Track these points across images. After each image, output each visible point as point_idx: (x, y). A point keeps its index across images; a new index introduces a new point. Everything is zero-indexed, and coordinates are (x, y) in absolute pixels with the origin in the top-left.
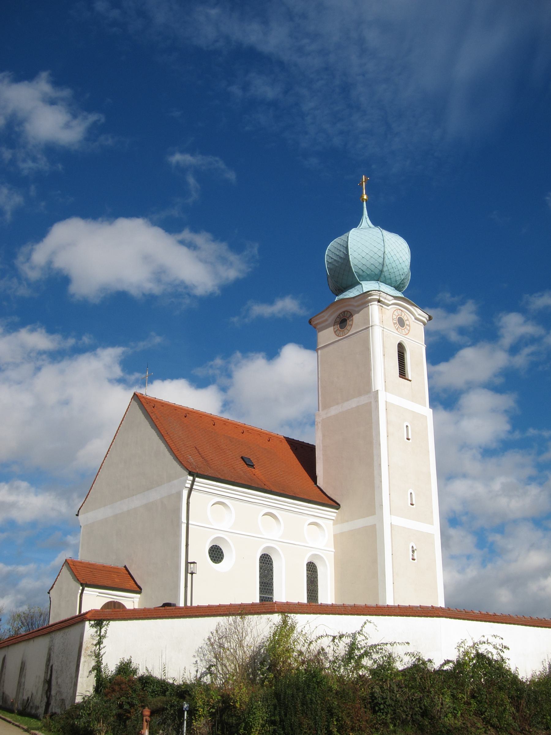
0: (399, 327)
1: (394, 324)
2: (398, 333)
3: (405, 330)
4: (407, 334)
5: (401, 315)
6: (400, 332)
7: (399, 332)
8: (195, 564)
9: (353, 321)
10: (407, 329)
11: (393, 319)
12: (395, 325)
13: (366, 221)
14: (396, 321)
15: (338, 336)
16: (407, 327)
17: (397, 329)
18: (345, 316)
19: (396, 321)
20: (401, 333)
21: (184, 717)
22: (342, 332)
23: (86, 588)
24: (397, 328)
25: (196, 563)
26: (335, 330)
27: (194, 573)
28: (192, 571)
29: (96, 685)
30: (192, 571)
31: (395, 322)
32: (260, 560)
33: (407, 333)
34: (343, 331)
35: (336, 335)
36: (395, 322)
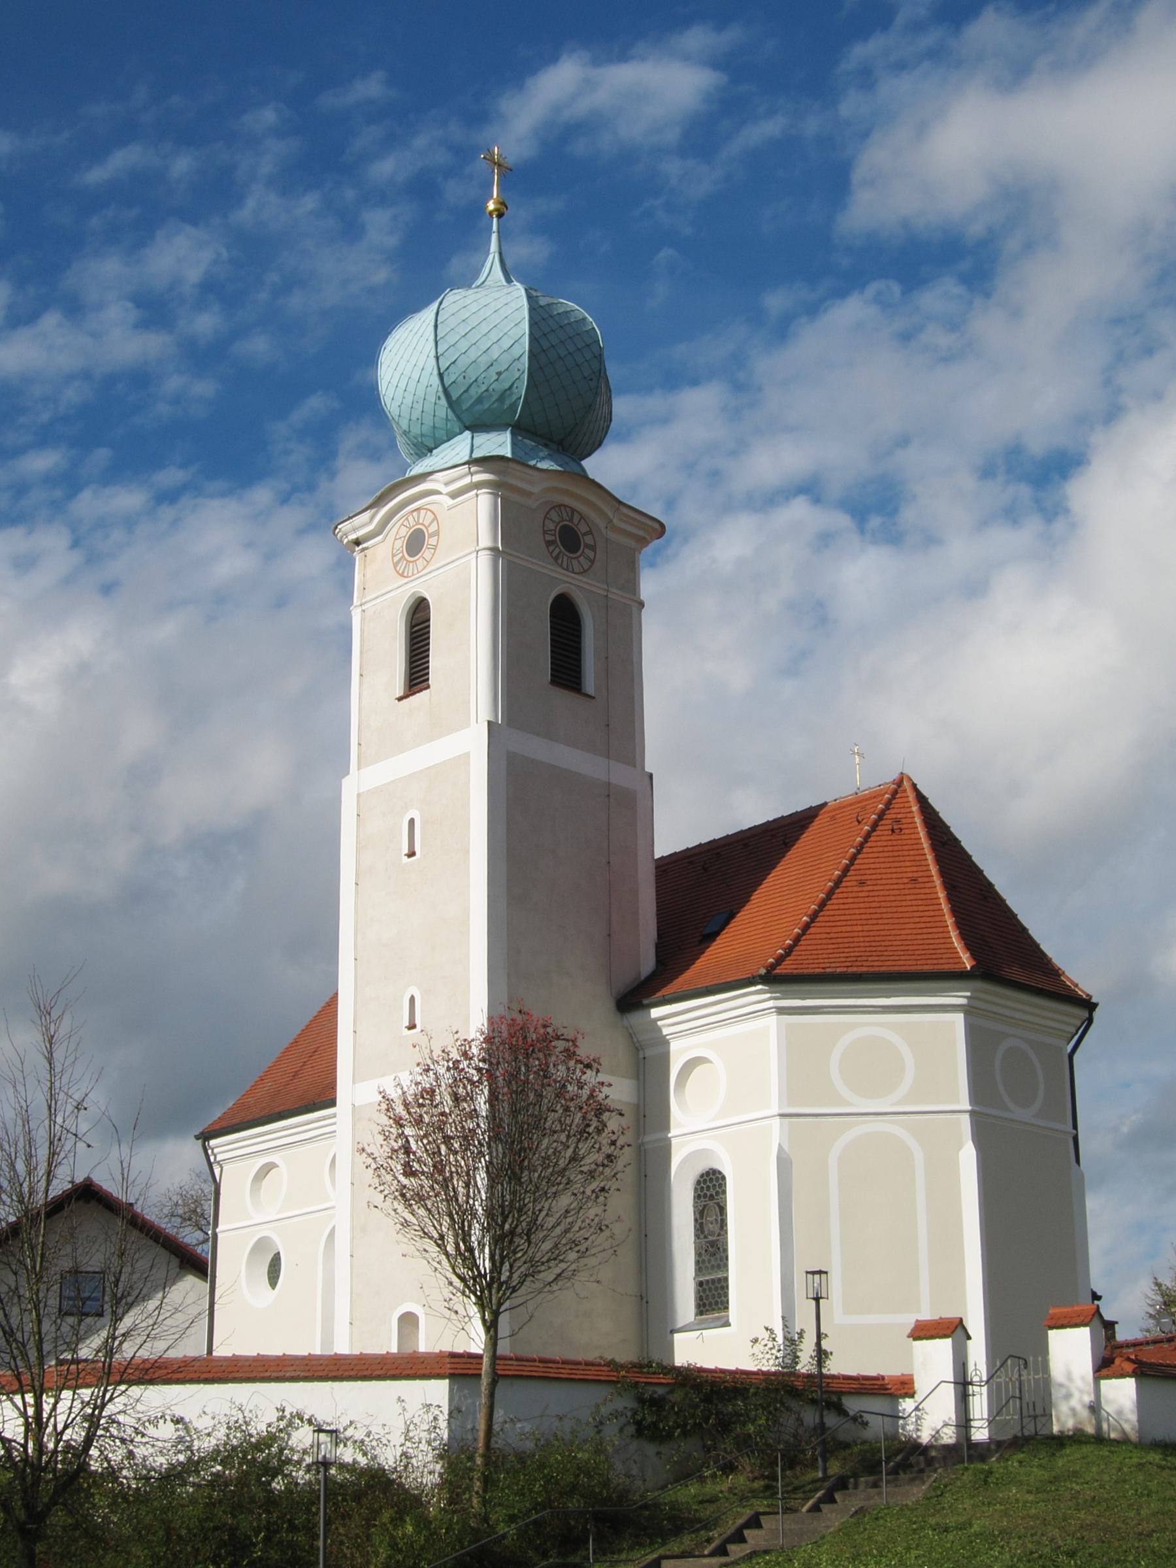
0: (560, 552)
1: (549, 543)
2: (562, 571)
3: (582, 559)
4: (585, 571)
5: (571, 520)
6: (565, 565)
7: (561, 566)
8: (823, 1276)
9: (438, 535)
10: (587, 558)
11: (545, 532)
12: (551, 548)
13: (492, 268)
14: (555, 535)
15: (402, 575)
16: (586, 551)
17: (556, 559)
18: (421, 521)
19: (555, 535)
20: (567, 569)
21: (40, 1231)
22: (411, 564)
23: (213, 1142)
24: (554, 554)
25: (826, 1273)
26: (396, 559)
27: (821, 1298)
28: (817, 1293)
29: (450, 1438)
30: (817, 1293)
31: (552, 538)
32: (696, 1190)
33: (586, 567)
34: (415, 561)
35: (398, 572)
36: (549, 538)
